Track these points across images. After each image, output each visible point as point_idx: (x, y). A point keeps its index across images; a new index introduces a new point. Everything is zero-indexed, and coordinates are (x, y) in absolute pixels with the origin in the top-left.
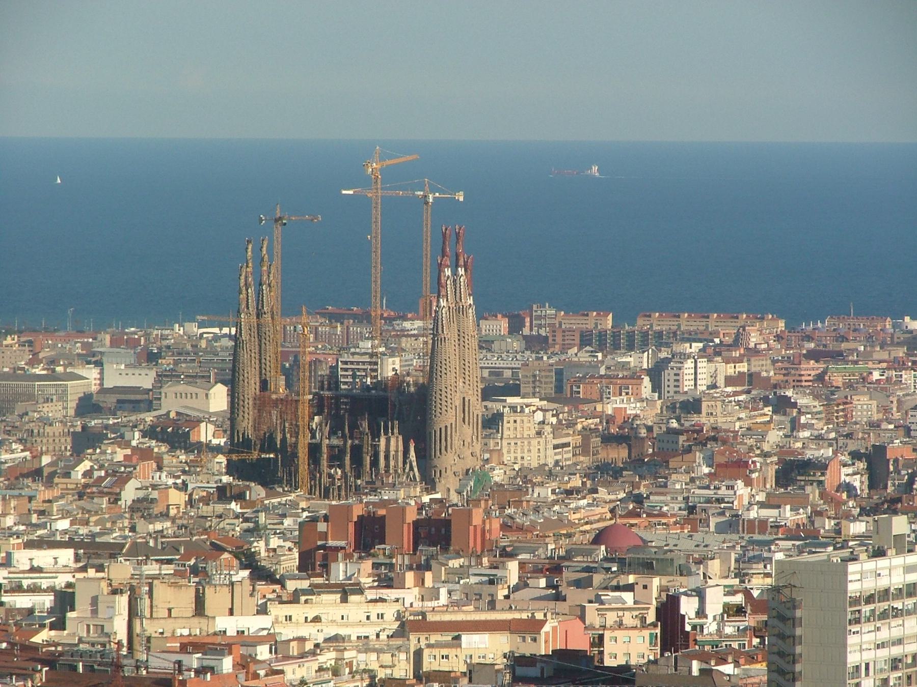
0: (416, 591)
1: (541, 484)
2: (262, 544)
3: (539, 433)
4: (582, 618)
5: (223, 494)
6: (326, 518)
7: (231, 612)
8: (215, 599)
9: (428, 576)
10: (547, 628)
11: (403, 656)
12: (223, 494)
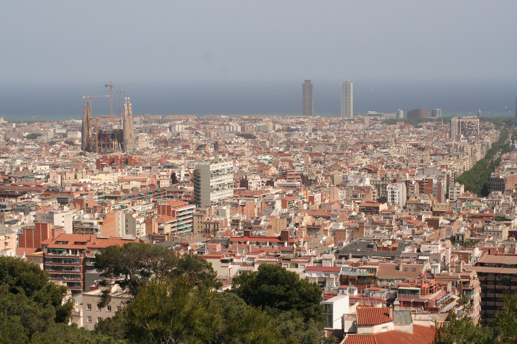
0: (121, 173)
1: (147, 151)
2: (89, 164)
3: (146, 140)
4: (155, 178)
5: (81, 154)
6: (102, 158)
7: (82, 178)
8: (79, 175)
9: (123, 170)
10: (148, 180)
11: (118, 186)
12: (81, 154)
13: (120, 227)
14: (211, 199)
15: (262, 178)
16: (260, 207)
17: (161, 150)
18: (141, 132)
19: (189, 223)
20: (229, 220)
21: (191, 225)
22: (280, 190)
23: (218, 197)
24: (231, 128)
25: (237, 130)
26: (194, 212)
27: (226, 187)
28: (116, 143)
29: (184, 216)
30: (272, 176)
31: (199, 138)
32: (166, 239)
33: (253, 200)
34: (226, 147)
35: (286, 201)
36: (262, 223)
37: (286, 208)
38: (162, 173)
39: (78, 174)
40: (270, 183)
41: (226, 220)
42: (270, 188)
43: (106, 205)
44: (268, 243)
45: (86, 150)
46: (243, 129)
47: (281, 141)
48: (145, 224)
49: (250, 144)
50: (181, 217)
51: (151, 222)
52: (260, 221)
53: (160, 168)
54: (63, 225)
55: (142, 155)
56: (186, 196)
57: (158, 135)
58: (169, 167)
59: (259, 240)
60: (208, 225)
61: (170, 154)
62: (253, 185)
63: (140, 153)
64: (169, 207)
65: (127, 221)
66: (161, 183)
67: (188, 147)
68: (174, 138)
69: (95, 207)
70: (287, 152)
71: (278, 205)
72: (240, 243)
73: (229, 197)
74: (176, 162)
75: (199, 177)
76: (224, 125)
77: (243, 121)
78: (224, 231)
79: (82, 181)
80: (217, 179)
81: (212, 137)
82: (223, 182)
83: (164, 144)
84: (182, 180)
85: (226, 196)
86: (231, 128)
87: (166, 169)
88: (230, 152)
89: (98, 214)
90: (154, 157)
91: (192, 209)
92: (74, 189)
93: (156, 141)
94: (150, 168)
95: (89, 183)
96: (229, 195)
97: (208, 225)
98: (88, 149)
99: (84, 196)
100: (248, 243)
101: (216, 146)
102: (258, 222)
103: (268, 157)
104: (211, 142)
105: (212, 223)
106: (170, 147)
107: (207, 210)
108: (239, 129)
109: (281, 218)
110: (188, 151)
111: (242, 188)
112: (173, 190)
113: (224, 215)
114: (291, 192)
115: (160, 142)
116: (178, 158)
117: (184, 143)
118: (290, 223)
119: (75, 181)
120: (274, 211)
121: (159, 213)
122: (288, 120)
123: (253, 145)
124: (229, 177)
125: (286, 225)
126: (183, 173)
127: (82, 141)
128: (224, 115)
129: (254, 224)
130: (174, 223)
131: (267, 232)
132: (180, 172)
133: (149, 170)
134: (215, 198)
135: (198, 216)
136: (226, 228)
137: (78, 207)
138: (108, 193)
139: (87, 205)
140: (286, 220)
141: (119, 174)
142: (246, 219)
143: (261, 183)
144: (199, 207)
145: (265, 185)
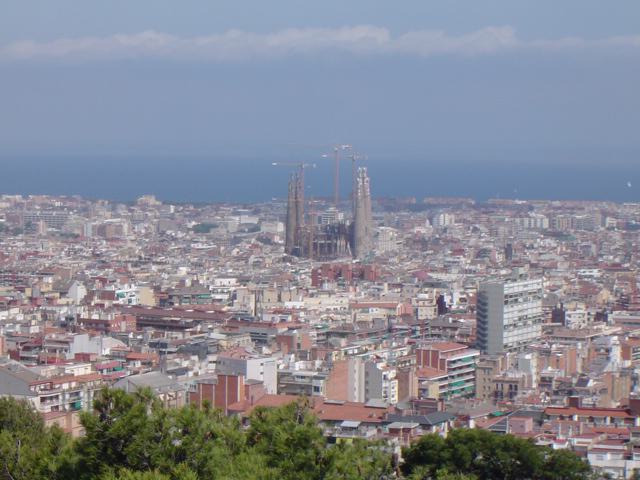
0: (353, 293)
3: (391, 239)
5: (284, 260)
6: (321, 268)
8: (285, 296)
10: (399, 306)
12: (284, 260)
13: (356, 385)
14: (505, 341)
15: (587, 307)
16: (586, 356)
17: (415, 256)
18: (382, 225)
19: (468, 381)
20: (534, 378)
21: (471, 384)
22: (618, 329)
23: (516, 339)
24: (532, 220)
25: (542, 224)
26: (477, 361)
27: (530, 322)
28: (343, 243)
29: (461, 368)
30: (604, 304)
31: (480, 237)
32: (439, 409)
33: (575, 345)
34: (525, 254)
35: (629, 347)
36: (591, 384)
37: (628, 359)
38: (422, 296)
39: (282, 294)
40: (601, 317)
41: (530, 376)
42: (603, 326)
43: (332, 347)
44: (608, 419)
45: (292, 254)
46: (552, 224)
47: (616, 246)
48: (397, 381)
49: (564, 249)
50: (454, 369)
51: (407, 379)
52: (587, 381)
53: (417, 286)
55: (385, 263)
56: (461, 335)
57: (411, 230)
58: (433, 285)
59: (595, 414)
60: (500, 386)
61: (433, 263)
62: (572, 319)
63: (383, 260)
64: (435, 353)
65: (367, 374)
66: (419, 313)
67: (461, 252)
68: (437, 236)
69: (314, 350)
70: (626, 265)
71: (616, 353)
72: (562, 418)
73: (534, 339)
74: (443, 277)
75: (485, 304)
76: (521, 217)
77: (552, 211)
78: (527, 396)
79: (289, 305)
81: (502, 236)
82: (525, 313)
83: (420, 247)
84: (454, 307)
85: (530, 336)
86: (532, 220)
87: (426, 289)
88: (533, 262)
89: (321, 362)
90: (406, 268)
91: (474, 357)
92: (278, 318)
93: (408, 239)
94: (400, 286)
95: (301, 310)
96: (534, 335)
97: (500, 386)
98: (295, 252)
99: (295, 331)
100: (576, 418)
101: (508, 251)
102: (583, 382)
103: (596, 273)
104: (500, 244)
105: (507, 382)
106: (430, 252)
107: (500, 359)
108: (546, 224)
109: (621, 376)
110: (462, 259)
111: (554, 324)
112: (440, 323)
113: (527, 368)
115: (414, 242)
116: (446, 269)
117: (454, 245)
118: (635, 384)
119: (278, 306)
120: (610, 365)
121: (419, 362)
122: (627, 210)
123: (569, 251)
125: (628, 388)
126: (457, 296)
127: (287, 239)
128: (520, 200)
129: (577, 385)
130: (446, 378)
131: (599, 399)
132: (451, 294)
133: (399, 290)
134: (510, 339)
135: (484, 369)
136: (530, 391)
137: (285, 348)
138: (332, 326)
139: (299, 345)
140: (628, 380)
141: (352, 296)
142: (563, 376)
143: (586, 317)
144: (485, 353)
145: (592, 320)
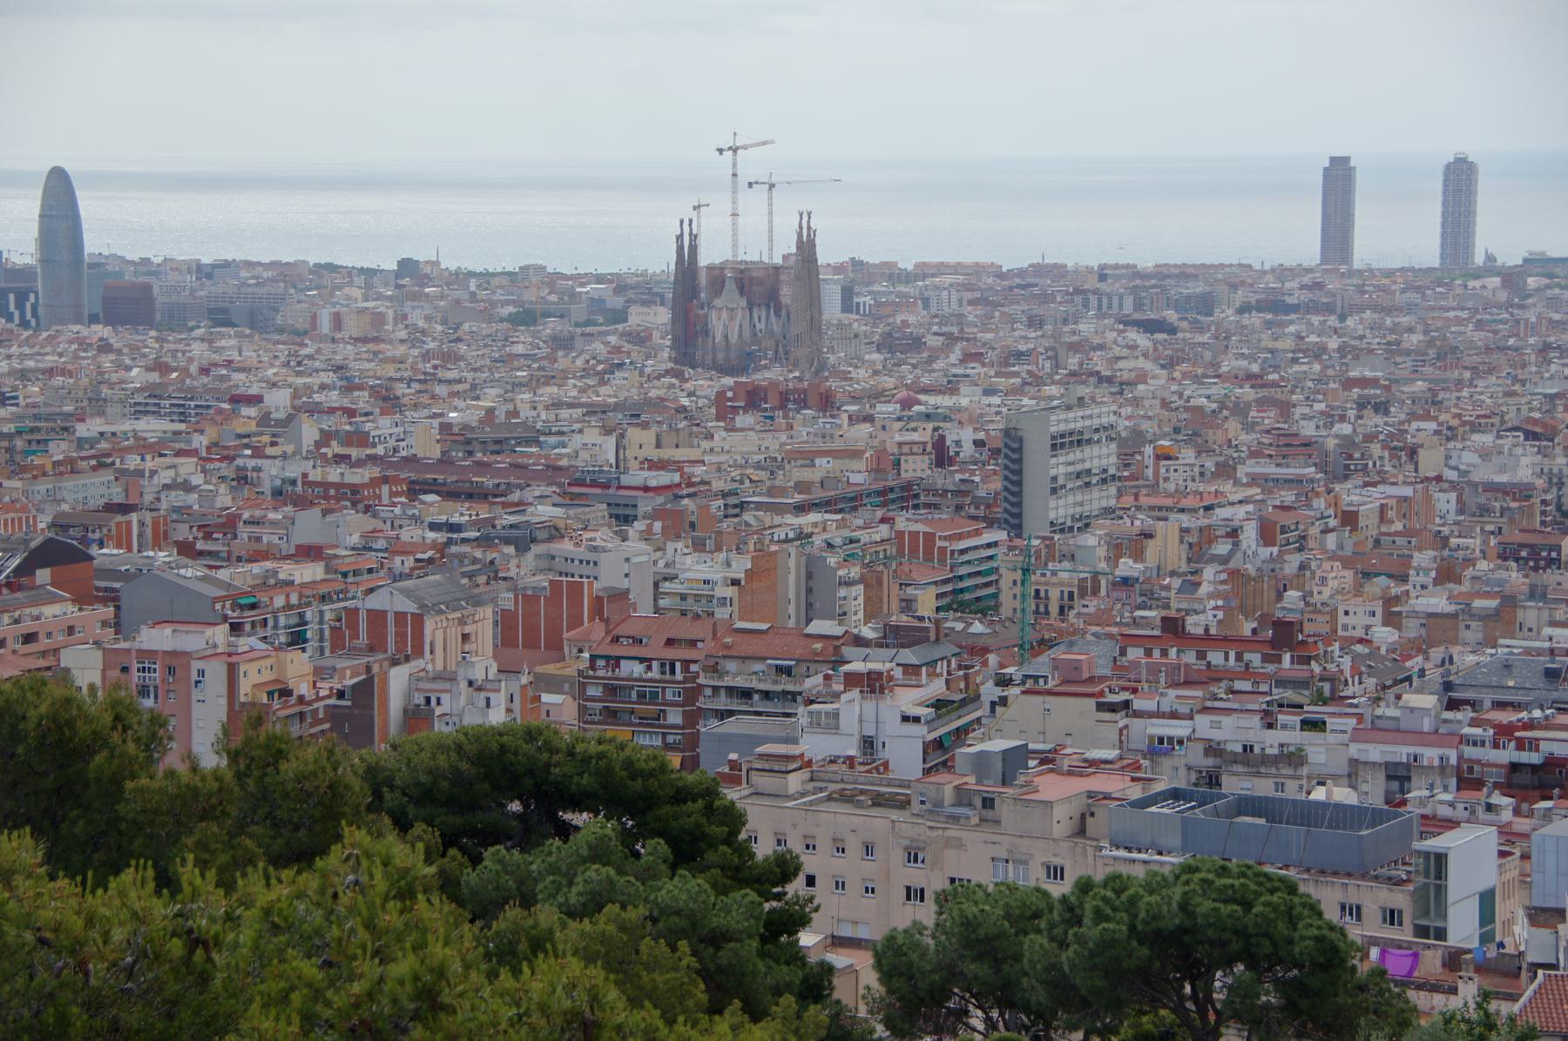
13: (792, 594)
22: (1255, 491)
40: (1226, 470)
48: (861, 587)
54: (625, 584)
55: (846, 379)
66: (903, 466)
80: (1071, 457)
99: (686, 501)
114: (1288, 497)
124: (1105, 451)
